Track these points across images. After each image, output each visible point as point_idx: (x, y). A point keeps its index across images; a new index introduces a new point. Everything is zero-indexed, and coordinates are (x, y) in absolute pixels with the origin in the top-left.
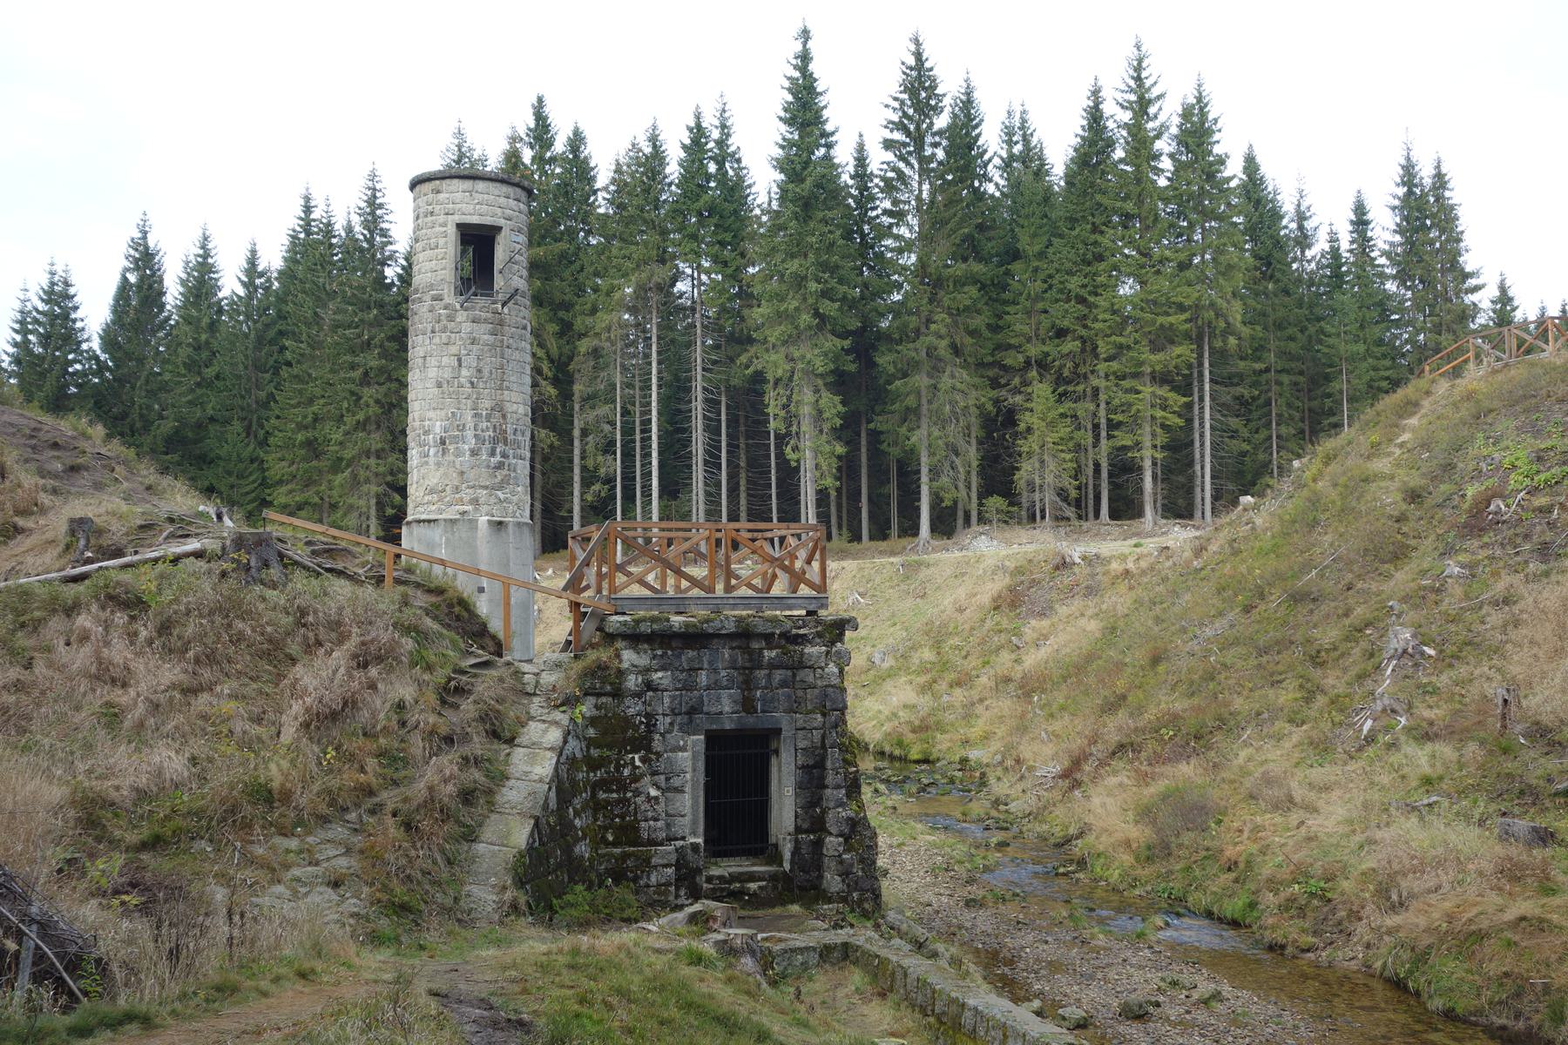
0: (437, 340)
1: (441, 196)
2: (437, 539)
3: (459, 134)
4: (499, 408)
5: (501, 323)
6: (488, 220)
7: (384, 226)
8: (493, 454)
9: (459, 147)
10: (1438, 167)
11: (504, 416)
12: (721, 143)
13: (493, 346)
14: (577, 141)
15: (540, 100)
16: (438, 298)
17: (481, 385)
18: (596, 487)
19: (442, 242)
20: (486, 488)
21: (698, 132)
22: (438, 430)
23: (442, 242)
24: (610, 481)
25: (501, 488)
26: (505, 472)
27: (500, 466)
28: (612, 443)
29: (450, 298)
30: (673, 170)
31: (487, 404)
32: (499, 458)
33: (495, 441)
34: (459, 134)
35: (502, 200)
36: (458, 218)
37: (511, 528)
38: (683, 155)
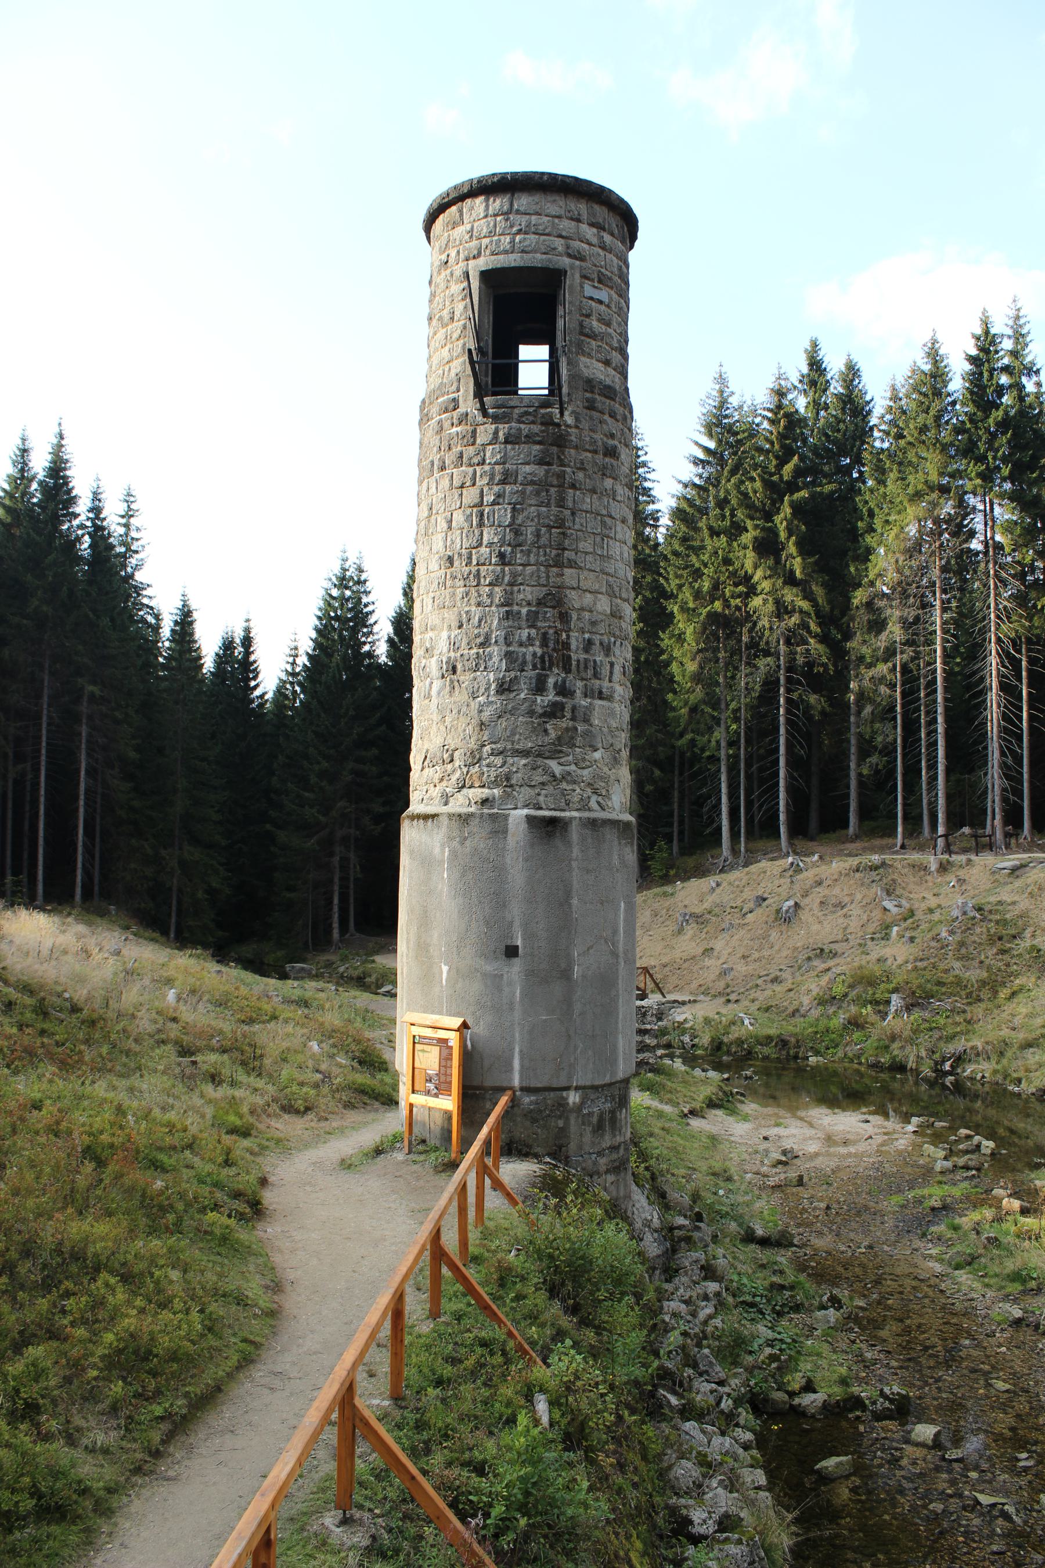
2: (437, 851)
3: (721, 380)
4: (554, 600)
5: (560, 441)
6: (537, 260)
7: (647, 484)
8: (540, 688)
9: (721, 392)
11: (564, 617)
12: (1015, 354)
13: (541, 486)
14: (852, 372)
15: (815, 345)
17: (520, 558)
18: (874, 759)
20: (525, 753)
21: (987, 343)
22: (442, 646)
24: (889, 751)
25: (555, 753)
26: (565, 723)
27: (554, 711)
28: (892, 708)
29: (469, 405)
30: (956, 385)
31: (528, 593)
32: (551, 696)
33: (544, 664)
34: (721, 380)
35: (566, 226)
36: (484, 263)
37: (574, 828)
38: (968, 367)
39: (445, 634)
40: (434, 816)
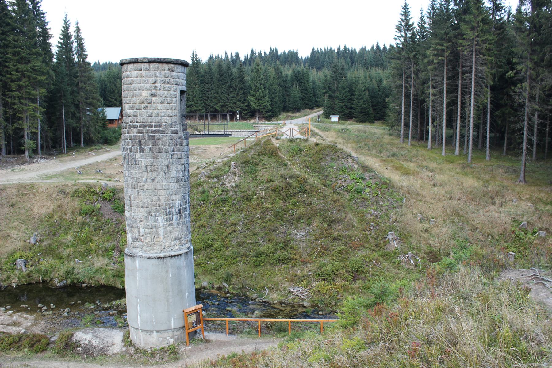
0: (175, 156)
1: (174, 74)
10: (77, 24)
16: (176, 133)
19: (174, 100)
22: (177, 206)
23: (174, 100)
39: (177, 202)
40: (180, 255)
